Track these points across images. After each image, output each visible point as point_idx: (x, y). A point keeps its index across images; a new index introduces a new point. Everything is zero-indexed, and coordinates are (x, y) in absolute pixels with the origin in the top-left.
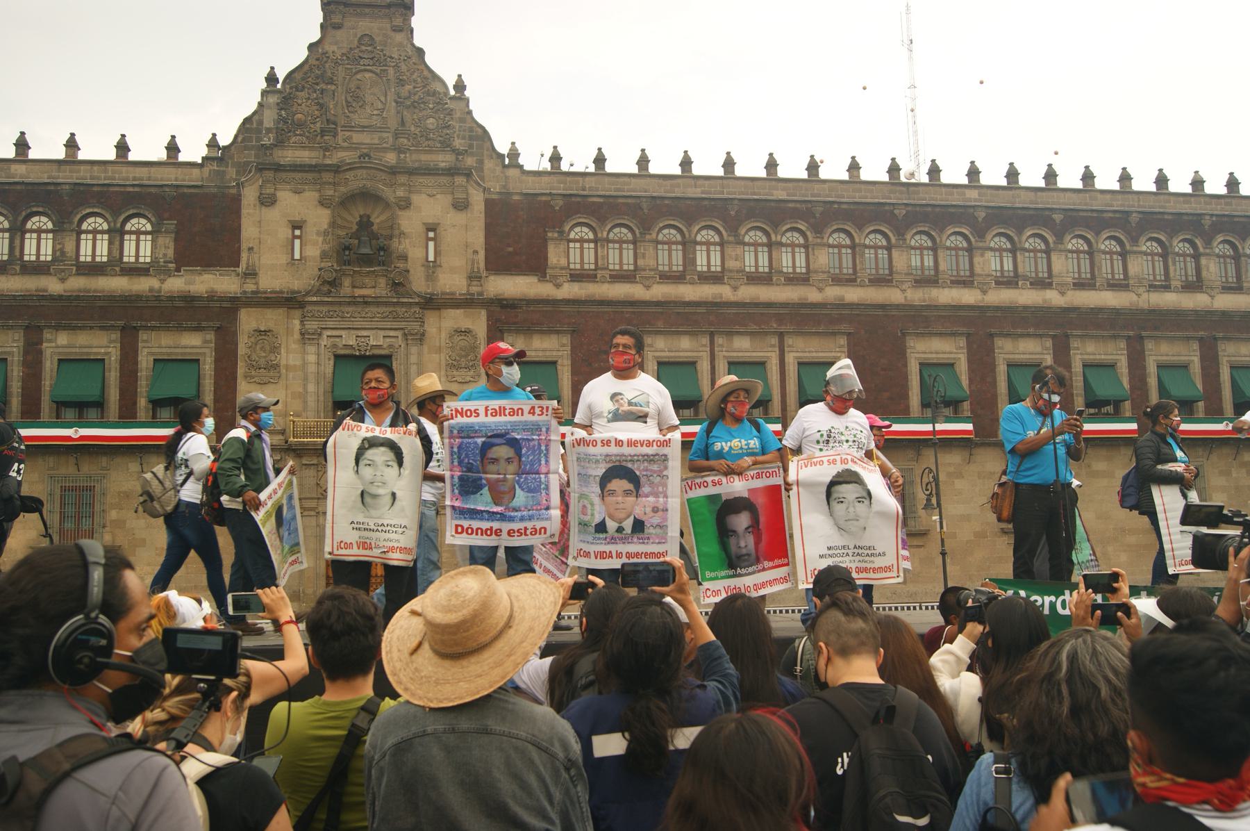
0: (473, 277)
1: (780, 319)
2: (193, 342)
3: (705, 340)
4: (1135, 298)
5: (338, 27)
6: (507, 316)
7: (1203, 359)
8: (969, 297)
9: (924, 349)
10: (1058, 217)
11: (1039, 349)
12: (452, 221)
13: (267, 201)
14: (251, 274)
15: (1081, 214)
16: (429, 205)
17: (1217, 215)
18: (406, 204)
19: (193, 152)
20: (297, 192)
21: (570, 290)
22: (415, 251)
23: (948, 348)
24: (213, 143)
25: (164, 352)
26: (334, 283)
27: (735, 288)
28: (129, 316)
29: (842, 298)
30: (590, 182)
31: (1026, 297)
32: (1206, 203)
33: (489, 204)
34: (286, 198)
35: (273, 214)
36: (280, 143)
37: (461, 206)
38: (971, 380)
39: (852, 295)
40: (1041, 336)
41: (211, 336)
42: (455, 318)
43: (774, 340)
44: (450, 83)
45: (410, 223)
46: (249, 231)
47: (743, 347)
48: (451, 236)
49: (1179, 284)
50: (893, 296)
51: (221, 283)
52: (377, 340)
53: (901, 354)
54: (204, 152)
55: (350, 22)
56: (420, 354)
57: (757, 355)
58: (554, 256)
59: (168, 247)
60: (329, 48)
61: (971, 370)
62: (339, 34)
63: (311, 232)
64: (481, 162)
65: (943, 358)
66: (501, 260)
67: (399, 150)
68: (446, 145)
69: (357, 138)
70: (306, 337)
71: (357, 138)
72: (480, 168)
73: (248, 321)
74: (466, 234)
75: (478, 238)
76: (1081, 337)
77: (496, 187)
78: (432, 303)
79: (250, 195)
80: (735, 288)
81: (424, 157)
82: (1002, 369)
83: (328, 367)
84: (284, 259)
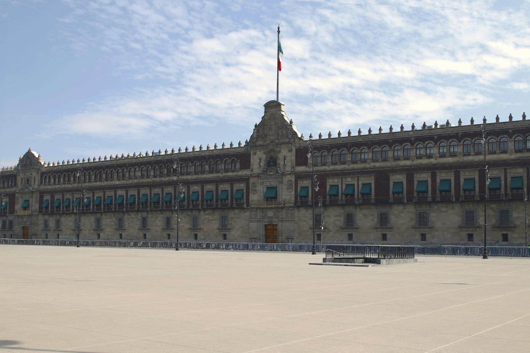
0: (293, 167)
1: (358, 173)
2: (242, 186)
3: (340, 179)
4: (458, 159)
5: (267, 112)
6: (299, 177)
7: (479, 176)
8: (408, 163)
9: (395, 178)
10: (435, 137)
12: (289, 154)
13: (255, 154)
14: (252, 170)
16: (284, 152)
18: (280, 152)
19: (243, 145)
20: (260, 151)
24: (246, 142)
25: (237, 188)
26: (266, 171)
27: (349, 165)
29: (374, 166)
30: (317, 142)
31: (425, 161)
33: (297, 150)
34: (258, 153)
35: (256, 157)
36: (257, 141)
37: (290, 151)
38: (407, 186)
39: (377, 165)
41: (245, 184)
42: (288, 177)
43: (356, 178)
44: (289, 122)
45: (281, 156)
46: (252, 161)
48: (288, 158)
49: (473, 153)
50: (388, 164)
52: (273, 183)
53: (388, 180)
54: (244, 144)
55: (270, 110)
56: (282, 186)
57: (352, 183)
59: (238, 166)
60: (266, 117)
62: (268, 114)
63: (262, 160)
64: (295, 140)
65: (399, 181)
66: (298, 164)
67: (278, 139)
68: (287, 137)
69: (271, 138)
70: (262, 183)
71: (271, 138)
72: (294, 142)
73: (252, 180)
74: (291, 157)
75: (294, 158)
77: (298, 146)
79: (252, 153)
80: (349, 165)
81: (283, 140)
82: (416, 183)
83: (265, 190)
84: (258, 166)
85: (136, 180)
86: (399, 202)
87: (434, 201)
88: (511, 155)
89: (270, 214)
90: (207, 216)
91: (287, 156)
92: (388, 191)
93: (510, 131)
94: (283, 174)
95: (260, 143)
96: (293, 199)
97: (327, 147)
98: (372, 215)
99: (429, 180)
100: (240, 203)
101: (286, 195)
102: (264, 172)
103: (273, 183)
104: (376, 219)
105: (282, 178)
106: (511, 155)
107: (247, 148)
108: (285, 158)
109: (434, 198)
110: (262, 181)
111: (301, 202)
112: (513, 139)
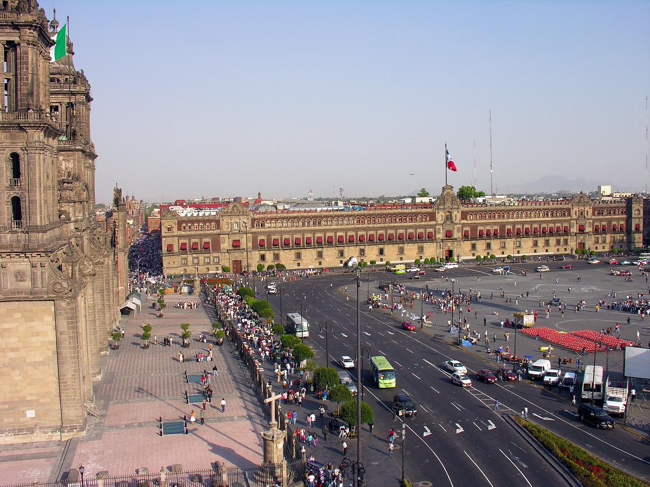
2: (431, 230)
6: (464, 225)
8: (513, 220)
16: (455, 213)
21: (470, 222)
22: (454, 218)
28: (425, 227)
31: (519, 220)
34: (441, 212)
37: (458, 212)
42: (458, 226)
47: (488, 228)
50: (504, 221)
51: (434, 223)
53: (505, 227)
58: (468, 218)
59: (428, 219)
66: (462, 219)
74: (459, 215)
78: (456, 224)
85: (352, 226)
86: (510, 237)
87: (523, 237)
89: (449, 244)
92: (505, 232)
96: (461, 237)
100: (431, 238)
101: (457, 235)
103: (449, 228)
107: (433, 210)
109: (523, 236)
111: (466, 237)
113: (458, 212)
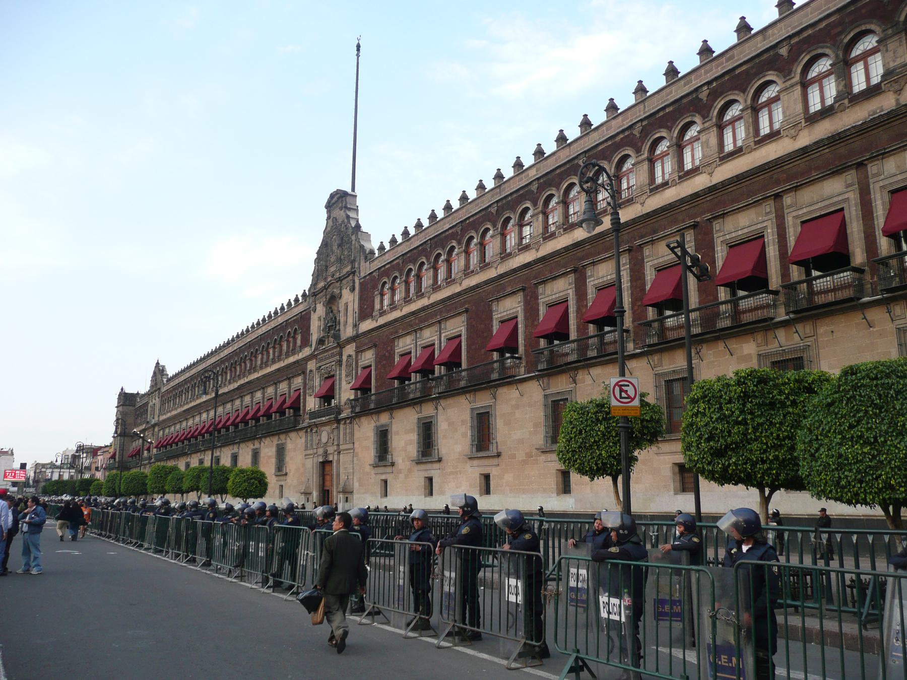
0: (356, 326)
11: (567, 286)
13: (315, 311)
15: (600, 148)
17: (716, 79)
23: (511, 306)
32: (706, 73)
38: (526, 326)
40: (565, 274)
46: (312, 328)
61: (526, 318)
64: (359, 264)
76: (594, 264)
77: (362, 275)
88: (794, 138)
90: (267, 450)
91: (349, 299)
93: (784, 51)
94: (341, 346)
95: (321, 284)
97: (398, 263)
98: (463, 422)
99: (571, 294)
101: (345, 393)
102: (321, 341)
103: (329, 364)
104: (469, 433)
105: (341, 355)
106: (794, 138)
108: (346, 305)
110: (318, 365)
112: (797, 78)
113: (353, 289)
